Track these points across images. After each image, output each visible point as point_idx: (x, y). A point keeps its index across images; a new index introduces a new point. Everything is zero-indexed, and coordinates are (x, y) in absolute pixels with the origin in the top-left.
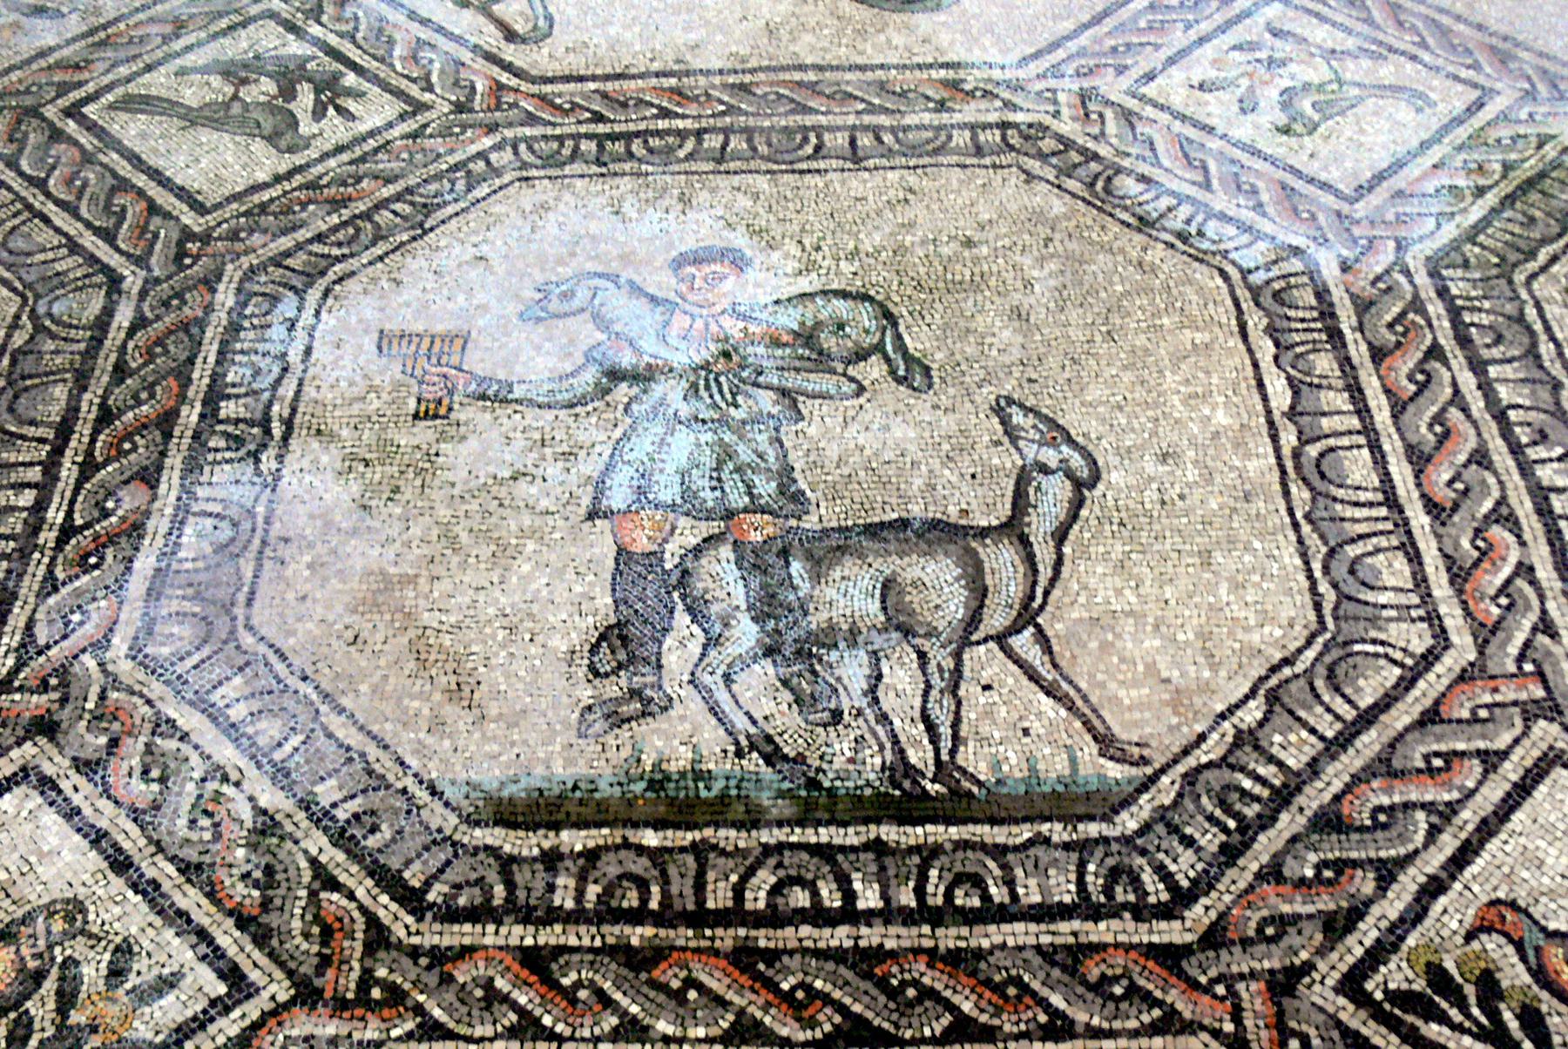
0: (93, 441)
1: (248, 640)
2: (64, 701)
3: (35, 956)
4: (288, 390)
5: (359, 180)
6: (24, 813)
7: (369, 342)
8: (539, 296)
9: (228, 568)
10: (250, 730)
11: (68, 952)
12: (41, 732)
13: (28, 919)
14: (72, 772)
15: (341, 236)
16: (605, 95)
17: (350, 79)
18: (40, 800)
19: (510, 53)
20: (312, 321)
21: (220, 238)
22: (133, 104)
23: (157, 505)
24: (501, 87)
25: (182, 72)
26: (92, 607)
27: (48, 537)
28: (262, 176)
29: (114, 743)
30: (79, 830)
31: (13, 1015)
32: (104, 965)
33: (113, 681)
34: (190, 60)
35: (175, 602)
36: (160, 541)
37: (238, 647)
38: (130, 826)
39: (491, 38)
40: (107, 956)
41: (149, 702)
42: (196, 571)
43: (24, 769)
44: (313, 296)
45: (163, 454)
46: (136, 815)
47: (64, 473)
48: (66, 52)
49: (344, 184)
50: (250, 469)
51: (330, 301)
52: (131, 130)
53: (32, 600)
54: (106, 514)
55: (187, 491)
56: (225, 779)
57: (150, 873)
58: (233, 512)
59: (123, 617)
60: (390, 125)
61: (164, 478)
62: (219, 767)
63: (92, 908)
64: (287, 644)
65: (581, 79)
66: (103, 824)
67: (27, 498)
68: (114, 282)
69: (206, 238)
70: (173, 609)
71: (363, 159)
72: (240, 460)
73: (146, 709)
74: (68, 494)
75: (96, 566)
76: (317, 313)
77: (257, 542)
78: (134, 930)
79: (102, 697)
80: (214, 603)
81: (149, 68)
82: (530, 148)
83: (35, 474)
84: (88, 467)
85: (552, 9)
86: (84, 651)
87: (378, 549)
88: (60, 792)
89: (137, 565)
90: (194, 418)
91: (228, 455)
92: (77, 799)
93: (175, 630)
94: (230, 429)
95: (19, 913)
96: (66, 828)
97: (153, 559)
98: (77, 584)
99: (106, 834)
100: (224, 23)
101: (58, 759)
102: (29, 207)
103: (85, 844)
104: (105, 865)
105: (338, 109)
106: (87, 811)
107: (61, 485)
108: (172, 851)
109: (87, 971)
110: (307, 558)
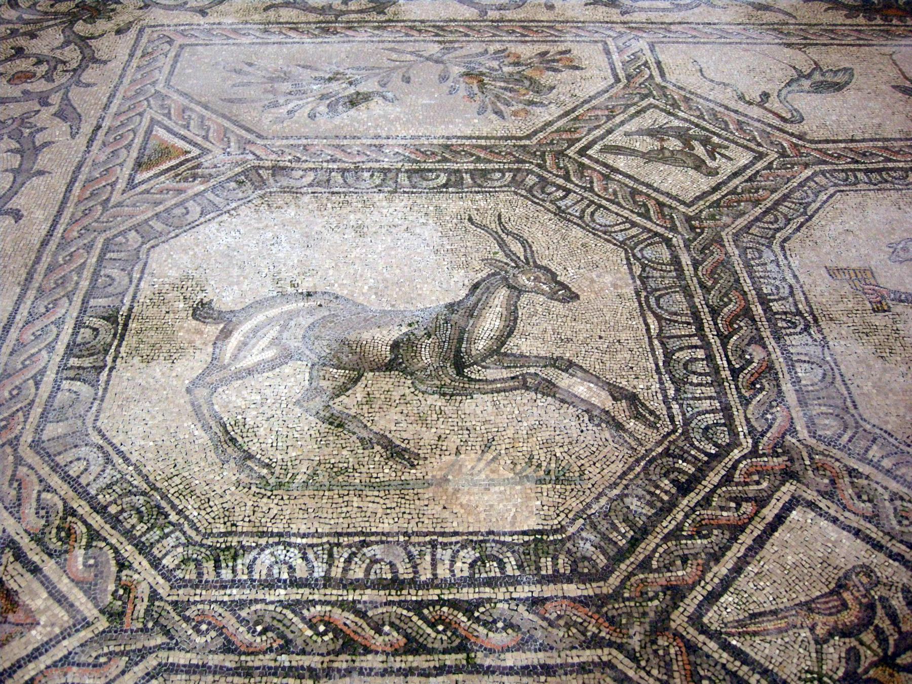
0: (716, 324)
1: (868, 427)
2: (791, 460)
3: (865, 596)
4: (800, 296)
5: (757, 192)
6: (809, 521)
7: (823, 271)
8: (891, 250)
9: (832, 390)
10: (899, 473)
11: (879, 593)
12: (791, 477)
13: (846, 576)
14: (820, 498)
15: (767, 219)
16: (851, 150)
17: (715, 139)
18: (813, 514)
19: (788, 127)
20: (785, 262)
21: (706, 219)
22: (617, 150)
23: (773, 356)
24: (796, 145)
25: (627, 134)
26: (774, 410)
27: (726, 374)
28: (706, 188)
29: (833, 482)
30: (844, 529)
31: (872, 628)
32: (901, 599)
33: (811, 451)
34: (627, 127)
35: (816, 407)
36: (787, 376)
37: (865, 430)
38: (869, 525)
39: (777, 122)
40: (900, 595)
41: (837, 460)
42: (817, 391)
43: (793, 496)
44: (776, 247)
45: (758, 329)
46: (869, 519)
47: (712, 341)
48: (560, 124)
49: (750, 192)
50: (808, 338)
51: (788, 253)
52: (621, 163)
53: (740, 407)
54: (750, 362)
55: (784, 350)
56: (902, 499)
57: (895, 550)
58: (815, 360)
59: (794, 415)
60: (752, 163)
61: (767, 343)
62: (895, 494)
63: (876, 570)
64: (889, 427)
65: (834, 142)
66: (854, 525)
67: (700, 354)
68: (668, 242)
69: (697, 217)
70: (819, 411)
71: (750, 179)
72: (800, 333)
73: (837, 464)
74: (721, 351)
75: (762, 389)
76: (786, 258)
77: (838, 378)
78: (905, 580)
79: (811, 459)
80: (837, 407)
81: (609, 132)
82: (832, 175)
83: (695, 341)
84: (724, 340)
85: (796, 107)
86: (784, 434)
87: (901, 380)
88: (821, 509)
89: (784, 388)
90: (760, 311)
91: (792, 330)
92: (832, 512)
93: (827, 422)
94: (784, 317)
95: (841, 574)
96: (836, 528)
97: (789, 385)
98: (758, 399)
99: (859, 531)
100: (632, 110)
101: (809, 491)
102: (592, 202)
103: (850, 535)
104: (869, 547)
105: (719, 153)
106: (842, 518)
107: (714, 346)
108: (899, 538)
109: (894, 602)
110: (870, 384)
